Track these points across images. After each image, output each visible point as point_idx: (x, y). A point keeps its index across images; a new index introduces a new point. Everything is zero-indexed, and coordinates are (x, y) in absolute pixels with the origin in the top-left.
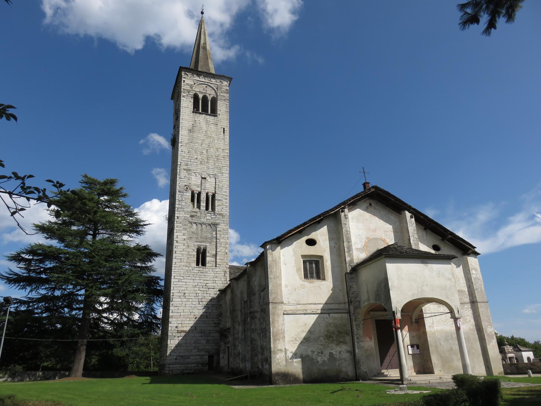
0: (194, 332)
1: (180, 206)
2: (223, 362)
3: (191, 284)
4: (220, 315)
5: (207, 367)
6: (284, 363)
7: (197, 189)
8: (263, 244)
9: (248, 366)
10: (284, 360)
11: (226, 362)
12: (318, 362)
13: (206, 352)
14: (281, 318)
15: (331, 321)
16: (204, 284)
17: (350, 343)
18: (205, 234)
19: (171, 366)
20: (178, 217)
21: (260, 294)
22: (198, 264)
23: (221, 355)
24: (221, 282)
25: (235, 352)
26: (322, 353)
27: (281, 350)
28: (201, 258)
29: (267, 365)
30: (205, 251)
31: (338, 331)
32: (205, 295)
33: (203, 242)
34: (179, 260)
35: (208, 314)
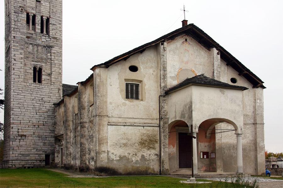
0: (33, 136)
1: (16, 27)
2: (58, 160)
3: (29, 97)
4: (55, 124)
5: (44, 163)
6: (106, 161)
7: (32, 12)
8: (93, 67)
9: (78, 163)
10: (107, 159)
11: (60, 160)
12: (132, 161)
13: (43, 152)
14: (105, 128)
15: (145, 132)
16: (41, 99)
17: (158, 149)
18: (40, 56)
19: (13, 161)
20: (14, 37)
21: (89, 108)
22: (35, 81)
23: (56, 155)
24: (55, 97)
25: (67, 152)
26: (136, 155)
27: (104, 152)
28: (38, 75)
29: (93, 162)
30: (40, 69)
31: (150, 140)
32: (41, 107)
33: (39, 62)
34: (18, 77)
35: (45, 123)
